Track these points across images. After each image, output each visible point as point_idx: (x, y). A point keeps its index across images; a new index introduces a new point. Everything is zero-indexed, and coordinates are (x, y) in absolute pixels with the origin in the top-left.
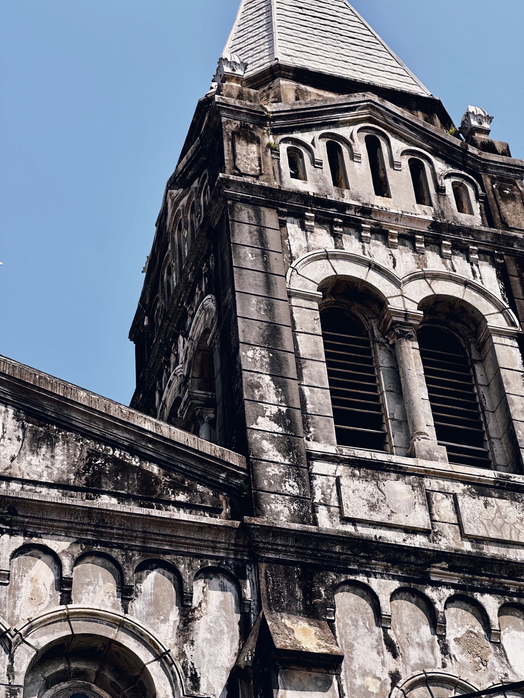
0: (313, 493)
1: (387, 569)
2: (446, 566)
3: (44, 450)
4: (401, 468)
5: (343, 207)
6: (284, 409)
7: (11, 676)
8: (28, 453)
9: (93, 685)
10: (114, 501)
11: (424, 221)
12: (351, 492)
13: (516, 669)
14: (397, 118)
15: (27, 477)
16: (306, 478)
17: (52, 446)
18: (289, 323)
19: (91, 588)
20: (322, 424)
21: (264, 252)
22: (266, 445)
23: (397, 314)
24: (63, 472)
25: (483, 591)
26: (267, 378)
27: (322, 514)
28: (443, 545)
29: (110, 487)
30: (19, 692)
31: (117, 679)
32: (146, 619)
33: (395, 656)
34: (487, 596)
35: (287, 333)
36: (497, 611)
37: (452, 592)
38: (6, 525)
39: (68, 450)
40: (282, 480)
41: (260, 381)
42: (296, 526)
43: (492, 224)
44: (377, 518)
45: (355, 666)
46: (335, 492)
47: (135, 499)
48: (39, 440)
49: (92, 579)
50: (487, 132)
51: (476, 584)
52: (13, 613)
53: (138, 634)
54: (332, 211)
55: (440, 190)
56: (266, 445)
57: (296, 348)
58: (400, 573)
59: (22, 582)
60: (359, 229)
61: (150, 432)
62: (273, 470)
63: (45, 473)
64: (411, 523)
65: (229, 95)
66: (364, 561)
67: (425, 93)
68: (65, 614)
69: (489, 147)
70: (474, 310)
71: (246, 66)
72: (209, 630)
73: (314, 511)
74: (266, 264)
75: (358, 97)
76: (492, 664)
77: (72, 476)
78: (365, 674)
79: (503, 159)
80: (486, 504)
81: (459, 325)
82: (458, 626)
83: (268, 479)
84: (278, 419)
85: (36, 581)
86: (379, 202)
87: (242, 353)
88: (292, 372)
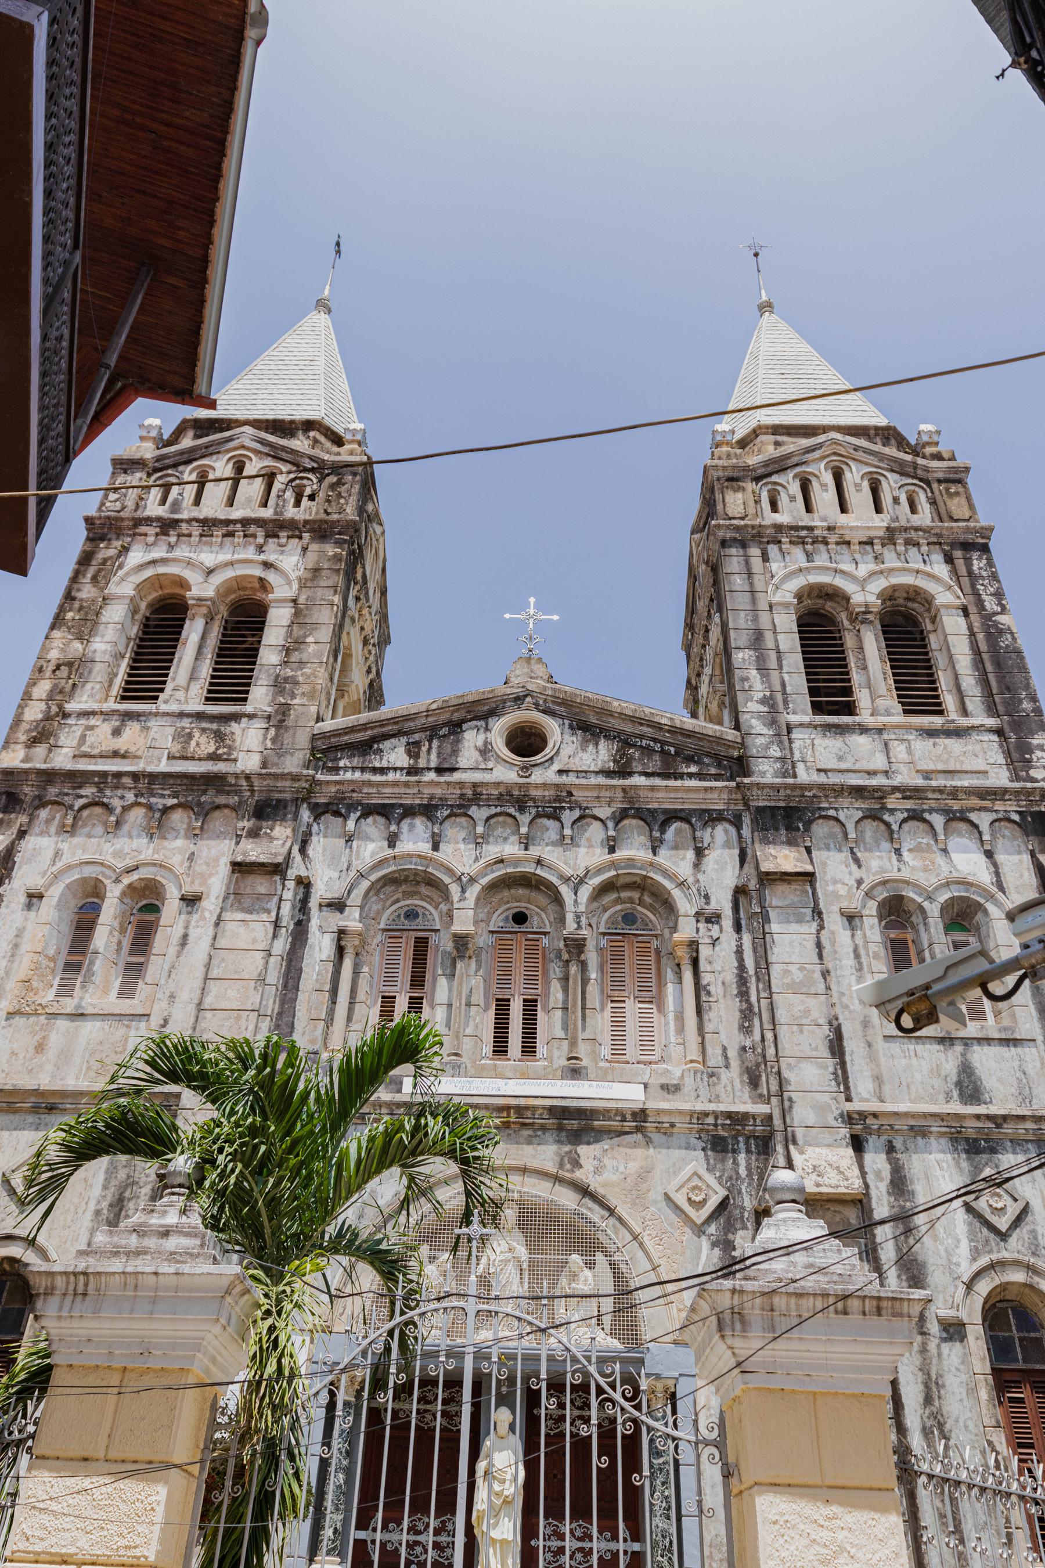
0: (792, 753)
3: (591, 747)
5: (810, 529)
6: (768, 694)
10: (643, 778)
11: (880, 527)
13: (959, 867)
14: (856, 448)
16: (786, 743)
17: (597, 744)
18: (770, 627)
20: (799, 701)
21: (750, 574)
22: (754, 722)
25: (931, 811)
26: (754, 672)
27: (800, 768)
28: (897, 781)
29: (640, 769)
33: (860, 867)
34: (934, 815)
35: (769, 636)
37: (906, 815)
40: (767, 747)
42: (778, 780)
43: (941, 520)
44: (844, 766)
45: (828, 877)
47: (659, 775)
50: (937, 444)
51: (925, 807)
54: (804, 533)
55: (896, 500)
56: (754, 722)
57: (778, 646)
60: (826, 543)
62: (760, 741)
64: (872, 767)
65: (720, 458)
67: (882, 421)
69: (938, 457)
70: (925, 591)
71: (733, 432)
72: (716, 862)
73: (794, 767)
74: (751, 584)
75: (821, 439)
78: (835, 882)
79: (952, 464)
80: (934, 745)
81: (915, 605)
83: (756, 747)
84: (763, 701)
86: (843, 519)
87: (734, 656)
88: (773, 663)
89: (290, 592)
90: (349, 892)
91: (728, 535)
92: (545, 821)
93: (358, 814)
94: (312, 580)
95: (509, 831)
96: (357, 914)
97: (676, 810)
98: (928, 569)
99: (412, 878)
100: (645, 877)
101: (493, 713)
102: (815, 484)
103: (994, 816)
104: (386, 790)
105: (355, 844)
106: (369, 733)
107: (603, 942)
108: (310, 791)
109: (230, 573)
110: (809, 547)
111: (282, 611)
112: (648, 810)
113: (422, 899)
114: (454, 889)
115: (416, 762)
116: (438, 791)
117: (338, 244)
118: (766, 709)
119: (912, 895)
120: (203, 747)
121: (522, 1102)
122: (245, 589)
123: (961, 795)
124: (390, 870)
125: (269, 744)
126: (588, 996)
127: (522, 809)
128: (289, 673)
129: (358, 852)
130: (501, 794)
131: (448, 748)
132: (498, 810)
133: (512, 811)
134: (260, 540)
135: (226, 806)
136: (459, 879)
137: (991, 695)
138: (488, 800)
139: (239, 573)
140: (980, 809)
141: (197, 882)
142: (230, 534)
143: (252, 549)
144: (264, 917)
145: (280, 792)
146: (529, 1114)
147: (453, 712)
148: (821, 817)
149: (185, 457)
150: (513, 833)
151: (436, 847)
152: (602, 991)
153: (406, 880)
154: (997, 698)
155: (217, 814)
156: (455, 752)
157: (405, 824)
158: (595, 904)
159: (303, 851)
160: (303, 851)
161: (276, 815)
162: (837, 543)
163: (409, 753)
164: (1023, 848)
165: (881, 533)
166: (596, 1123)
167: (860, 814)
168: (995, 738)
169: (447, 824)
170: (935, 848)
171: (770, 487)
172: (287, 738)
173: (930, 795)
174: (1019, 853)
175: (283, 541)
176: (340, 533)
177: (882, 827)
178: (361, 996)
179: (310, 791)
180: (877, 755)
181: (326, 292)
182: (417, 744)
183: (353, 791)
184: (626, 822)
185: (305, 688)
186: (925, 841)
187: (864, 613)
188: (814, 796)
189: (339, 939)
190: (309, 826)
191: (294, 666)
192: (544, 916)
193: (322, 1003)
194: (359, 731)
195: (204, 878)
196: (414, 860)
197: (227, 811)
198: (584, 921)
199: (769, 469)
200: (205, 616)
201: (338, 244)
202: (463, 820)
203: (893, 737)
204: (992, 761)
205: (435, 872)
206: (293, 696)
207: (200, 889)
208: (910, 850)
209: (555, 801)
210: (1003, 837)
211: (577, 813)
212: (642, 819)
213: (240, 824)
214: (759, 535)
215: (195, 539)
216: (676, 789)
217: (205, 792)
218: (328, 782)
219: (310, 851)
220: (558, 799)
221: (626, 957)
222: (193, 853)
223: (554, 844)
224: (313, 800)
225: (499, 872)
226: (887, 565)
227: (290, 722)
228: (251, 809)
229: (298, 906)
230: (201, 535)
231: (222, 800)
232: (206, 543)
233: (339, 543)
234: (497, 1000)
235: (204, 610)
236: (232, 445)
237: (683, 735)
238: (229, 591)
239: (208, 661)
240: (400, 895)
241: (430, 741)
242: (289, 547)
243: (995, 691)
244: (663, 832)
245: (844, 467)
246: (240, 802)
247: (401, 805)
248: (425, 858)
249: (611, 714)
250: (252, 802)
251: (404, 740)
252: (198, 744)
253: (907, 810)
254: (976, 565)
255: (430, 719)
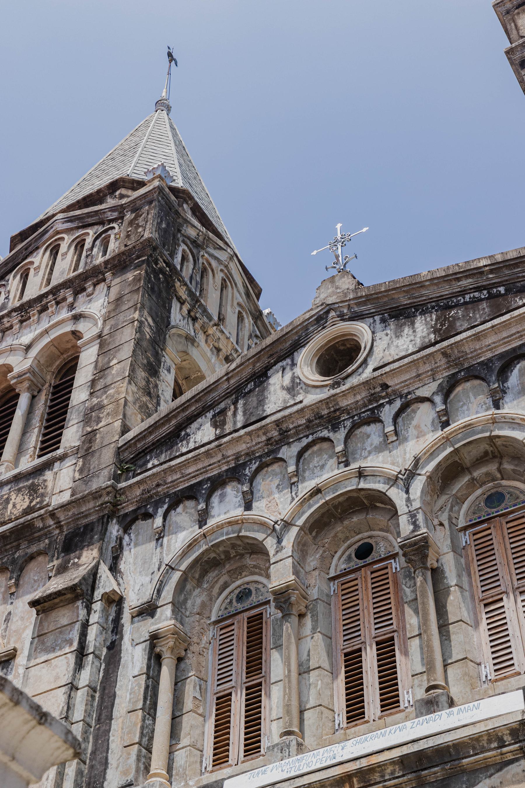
3: (407, 330)
7: (409, 505)
8: (394, 340)
9: (503, 481)
15: (397, 357)
17: (413, 323)
19: (465, 408)
24: (424, 337)
29: (466, 325)
30: (418, 513)
31: (516, 465)
32: (518, 406)
38: (385, 399)
39: (426, 320)
48: (401, 326)
49: (465, 401)
52: (404, 458)
53: (511, 421)
59: (408, 433)
61: (486, 266)
63: (411, 346)
68: (443, 438)
77: (432, 336)
85: (419, 427)
89: (95, 331)
90: (159, 592)
92: (366, 429)
93: (166, 506)
94: (114, 310)
95: (325, 456)
96: (168, 611)
97: (514, 349)
99: (233, 553)
100: (491, 438)
101: (297, 346)
104: (191, 470)
105: (165, 539)
106: (173, 422)
107: (465, 539)
108: (115, 505)
109: (46, 340)
111: (91, 349)
112: (481, 364)
113: (252, 574)
114: (270, 544)
115: (223, 429)
116: (242, 447)
117: (170, 55)
120: (18, 506)
121: (364, 763)
122: (66, 350)
124: (201, 551)
125: (77, 476)
126: (449, 608)
127: (335, 428)
128: (95, 401)
129: (169, 546)
130: (309, 421)
131: (253, 400)
132: (310, 438)
133: (325, 433)
134: (70, 300)
135: (39, 553)
136: (274, 529)
138: (297, 433)
139: (52, 337)
141: (12, 640)
142: (45, 309)
143: (65, 310)
144: (67, 650)
145: (86, 516)
146: (377, 777)
147: (254, 364)
149: (10, 265)
150: (331, 457)
151: (248, 506)
152: (473, 597)
153: (228, 558)
155: (32, 565)
156: (261, 402)
157: (215, 499)
158: (444, 498)
159: (114, 569)
160: (114, 569)
161: (82, 541)
163: (215, 425)
166: (465, 761)
169: (259, 478)
172: (94, 463)
175: (90, 290)
176: (138, 257)
178: (188, 704)
179: (115, 505)
181: (164, 94)
182: (223, 412)
183: (158, 485)
184: (459, 389)
185: (109, 409)
189: (152, 647)
190: (120, 540)
191: (99, 393)
192: (391, 537)
193: (135, 724)
194: (163, 424)
195: (19, 633)
196: (225, 530)
197: (40, 559)
198: (420, 517)
200: (29, 389)
201: (170, 55)
202: (276, 467)
205: (248, 534)
206: (99, 420)
207: (11, 646)
209: (370, 402)
211: (398, 404)
212: (477, 377)
213: (51, 564)
215: (16, 327)
216: (506, 325)
217: (18, 548)
218: (130, 486)
219: (122, 566)
220: (373, 398)
221: (495, 546)
222: (10, 613)
223: (379, 449)
224: (122, 513)
225: (319, 502)
227: (96, 446)
228: (60, 547)
229: (111, 626)
230: (21, 322)
231: (34, 549)
232: (26, 327)
233: (137, 267)
234: (346, 655)
235: (26, 384)
236: (47, 236)
237: (509, 267)
238: (51, 359)
239: (36, 430)
240: (224, 578)
241: (235, 403)
242: (96, 292)
244: (505, 379)
246: (50, 544)
247: (209, 479)
248: (236, 522)
249: (421, 285)
250: (61, 538)
251: (210, 415)
252: (14, 506)
255: (232, 381)
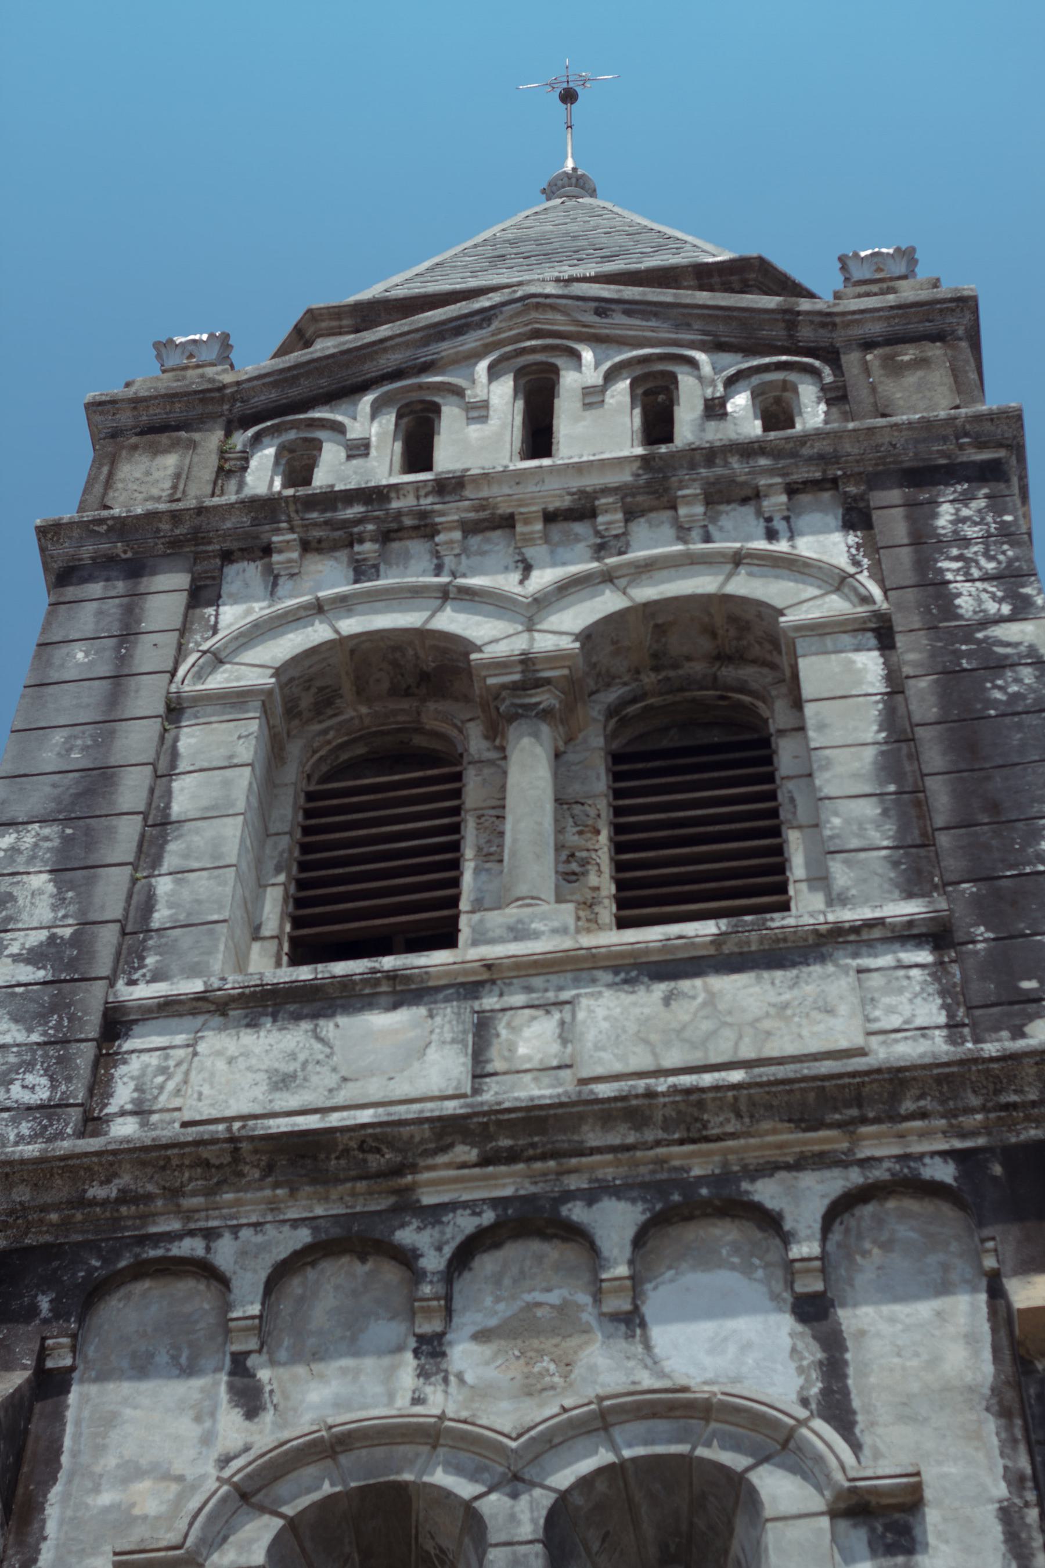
1: (273, 1205)
2: (472, 1154)
4: (408, 979)
6: (67, 932)
12: (221, 1065)
13: (668, 1365)
14: (603, 307)
23: (501, 665)
25: (591, 1197)
26: (40, 881)
36: (630, 1233)
37: (488, 1217)
41: (16, 891)
45: (110, 1461)
46: (178, 1077)
51: (574, 1182)
54: (355, 511)
58: (319, 1211)
66: (198, 1201)
74: (122, 660)
76: (592, 1369)
78: (131, 1472)
80: (667, 1000)
81: (747, 673)
82: (498, 1300)
91: (88, 551)
98: (782, 546)
102: (450, 415)
103: (855, 1177)
110: (368, 548)
118: (41, 975)
119: (441, 1477)
123: (718, 1122)
137: (927, 842)
140: (800, 1164)
148: (142, 1270)
154: (944, 840)
162: (470, 528)
164: (961, 1268)
165: (625, 477)
167: (304, 1236)
168: (925, 956)
170: (588, 1316)
171: (292, 435)
173: (593, 1138)
174: (944, 1288)
177: (391, 1273)
180: (432, 1054)
186: (554, 1297)
187: (516, 688)
188: (125, 1197)
199: (294, 393)
203: (518, 999)
204: (896, 1022)
208: (482, 1336)
210: (886, 1246)
214: (197, 537)
226: (638, 554)
243: (939, 821)
245: (559, 362)
253: (495, 1203)
254: (945, 516)
